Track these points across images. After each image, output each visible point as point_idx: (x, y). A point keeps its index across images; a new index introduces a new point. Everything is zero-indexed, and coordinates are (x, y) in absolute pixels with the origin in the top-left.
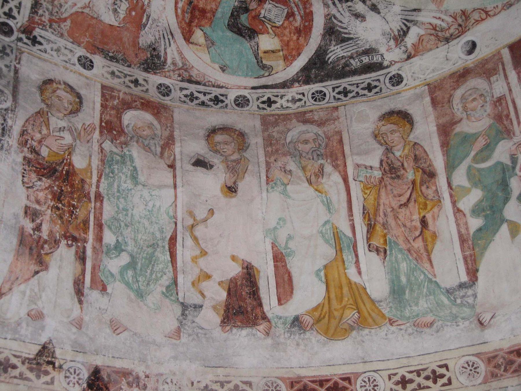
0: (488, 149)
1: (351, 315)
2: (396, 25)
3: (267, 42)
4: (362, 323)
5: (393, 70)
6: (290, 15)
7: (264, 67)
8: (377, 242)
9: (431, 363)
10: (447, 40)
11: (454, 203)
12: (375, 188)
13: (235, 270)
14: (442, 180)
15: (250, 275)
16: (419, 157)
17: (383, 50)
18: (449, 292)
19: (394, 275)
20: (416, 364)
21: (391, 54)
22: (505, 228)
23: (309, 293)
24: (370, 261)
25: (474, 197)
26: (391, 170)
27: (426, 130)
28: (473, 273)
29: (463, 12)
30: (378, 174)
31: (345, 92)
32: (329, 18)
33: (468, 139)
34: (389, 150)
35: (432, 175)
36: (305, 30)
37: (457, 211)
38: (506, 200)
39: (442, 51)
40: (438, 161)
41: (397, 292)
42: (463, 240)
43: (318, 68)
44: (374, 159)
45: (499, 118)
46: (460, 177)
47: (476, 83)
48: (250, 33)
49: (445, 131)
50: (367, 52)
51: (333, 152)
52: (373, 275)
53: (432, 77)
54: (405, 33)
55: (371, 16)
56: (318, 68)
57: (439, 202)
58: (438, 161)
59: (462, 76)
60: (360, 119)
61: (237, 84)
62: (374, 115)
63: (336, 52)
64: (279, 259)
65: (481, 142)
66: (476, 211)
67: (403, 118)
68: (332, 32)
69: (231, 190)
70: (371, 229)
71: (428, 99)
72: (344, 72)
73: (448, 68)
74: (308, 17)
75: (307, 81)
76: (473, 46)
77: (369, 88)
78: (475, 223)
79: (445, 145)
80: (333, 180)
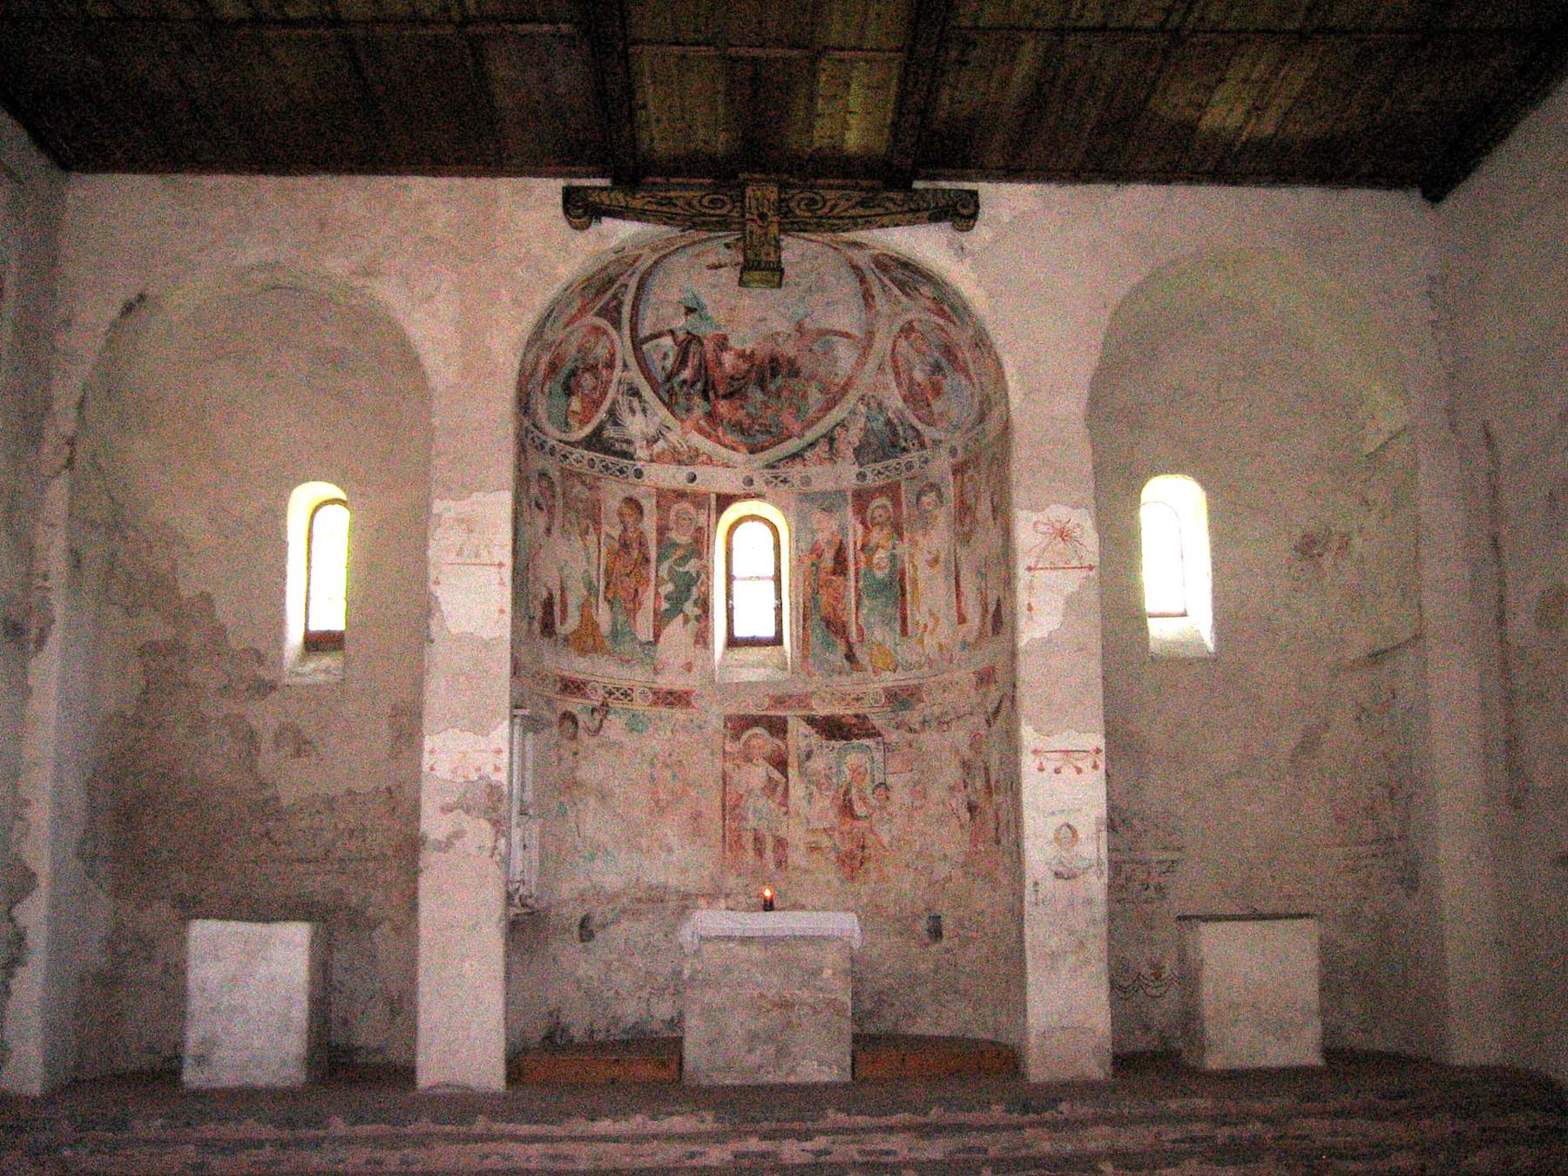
0: (684, 560)
1: (590, 641)
2: (652, 431)
3: (576, 404)
4: (595, 649)
5: (639, 465)
6: (595, 388)
7: (567, 424)
8: (610, 597)
9: (625, 685)
10: (680, 463)
11: (657, 586)
12: (615, 555)
13: (545, 594)
14: (653, 565)
15: (551, 597)
16: (642, 544)
17: (637, 445)
18: (641, 644)
19: (614, 624)
20: (618, 684)
21: (642, 453)
22: (681, 617)
23: (573, 623)
24: (604, 608)
25: (670, 587)
26: (625, 545)
27: (649, 525)
28: (657, 636)
29: (697, 450)
30: (617, 545)
31: (606, 468)
32: (613, 403)
33: (675, 545)
34: (625, 530)
35: (647, 561)
36: (597, 404)
37: (657, 594)
38: (687, 599)
39: (673, 468)
40: (653, 553)
41: (615, 634)
42: (656, 614)
43: (595, 441)
44: (616, 533)
45: (697, 541)
46: (664, 573)
47: (686, 505)
48: (568, 391)
49: (662, 530)
50: (629, 442)
51: (593, 514)
52: (603, 616)
53: (666, 485)
54: (656, 441)
55: (639, 415)
56: (595, 441)
57: (648, 581)
58: (653, 553)
59: (681, 495)
60: (613, 493)
61: (553, 434)
62: (620, 496)
63: (610, 432)
64: (563, 590)
65: (680, 552)
66: (668, 598)
67: (633, 504)
68: (611, 412)
69: (548, 531)
70: (607, 587)
71: (654, 501)
72: (607, 449)
73: (675, 485)
74: (604, 394)
75: (588, 448)
76: (693, 479)
77: (621, 471)
78: (665, 605)
79: (659, 542)
80: (592, 537)
